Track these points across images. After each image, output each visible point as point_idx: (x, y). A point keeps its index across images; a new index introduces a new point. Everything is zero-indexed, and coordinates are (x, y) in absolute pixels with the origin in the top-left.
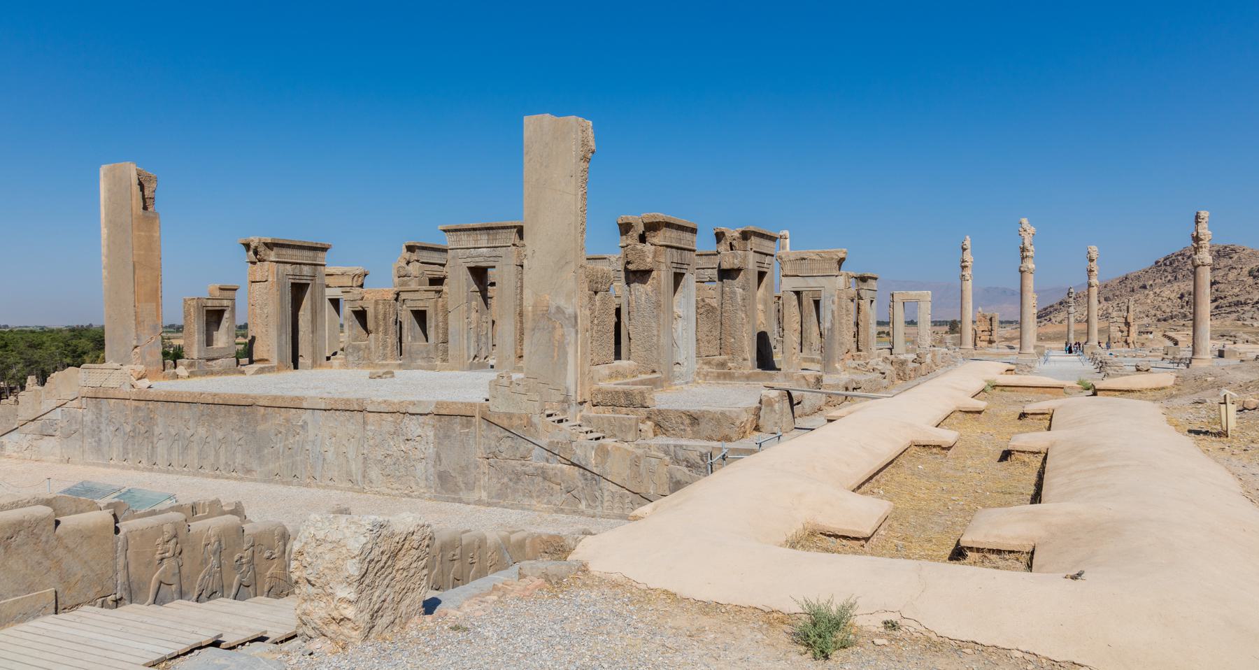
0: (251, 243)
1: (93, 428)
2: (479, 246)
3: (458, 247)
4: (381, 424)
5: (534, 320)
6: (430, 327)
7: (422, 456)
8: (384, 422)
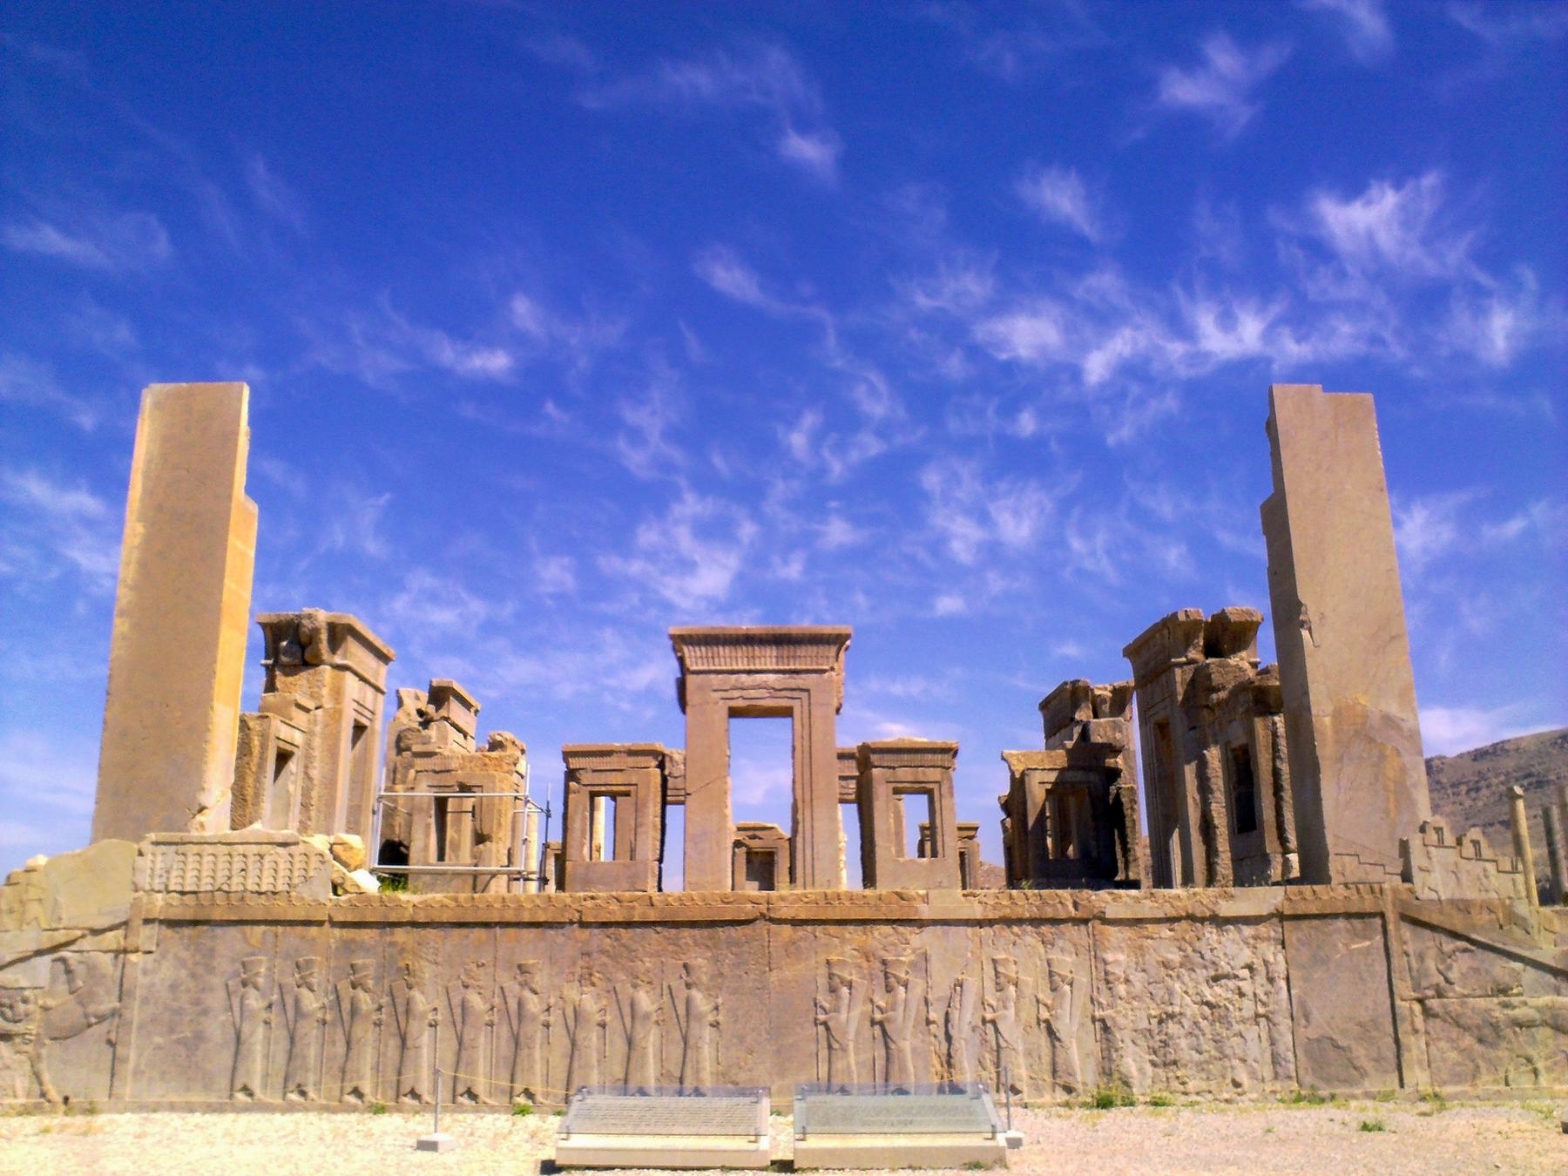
0: (305, 622)
1: (175, 1005)
2: (758, 667)
3: (713, 668)
4: (1141, 948)
5: (1337, 742)
6: (641, 825)
7: (1261, 1010)
8: (1149, 941)
